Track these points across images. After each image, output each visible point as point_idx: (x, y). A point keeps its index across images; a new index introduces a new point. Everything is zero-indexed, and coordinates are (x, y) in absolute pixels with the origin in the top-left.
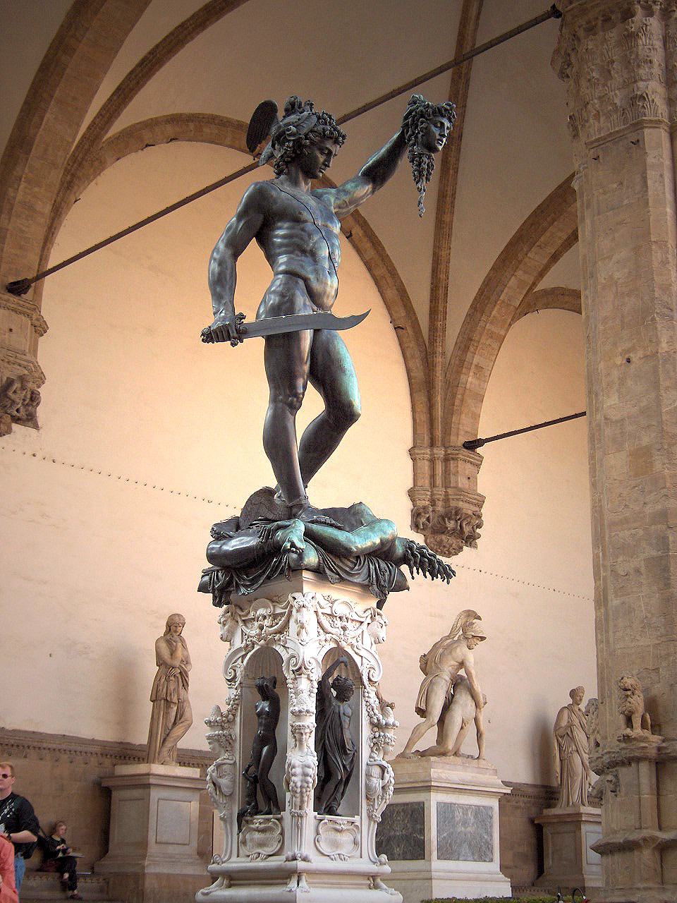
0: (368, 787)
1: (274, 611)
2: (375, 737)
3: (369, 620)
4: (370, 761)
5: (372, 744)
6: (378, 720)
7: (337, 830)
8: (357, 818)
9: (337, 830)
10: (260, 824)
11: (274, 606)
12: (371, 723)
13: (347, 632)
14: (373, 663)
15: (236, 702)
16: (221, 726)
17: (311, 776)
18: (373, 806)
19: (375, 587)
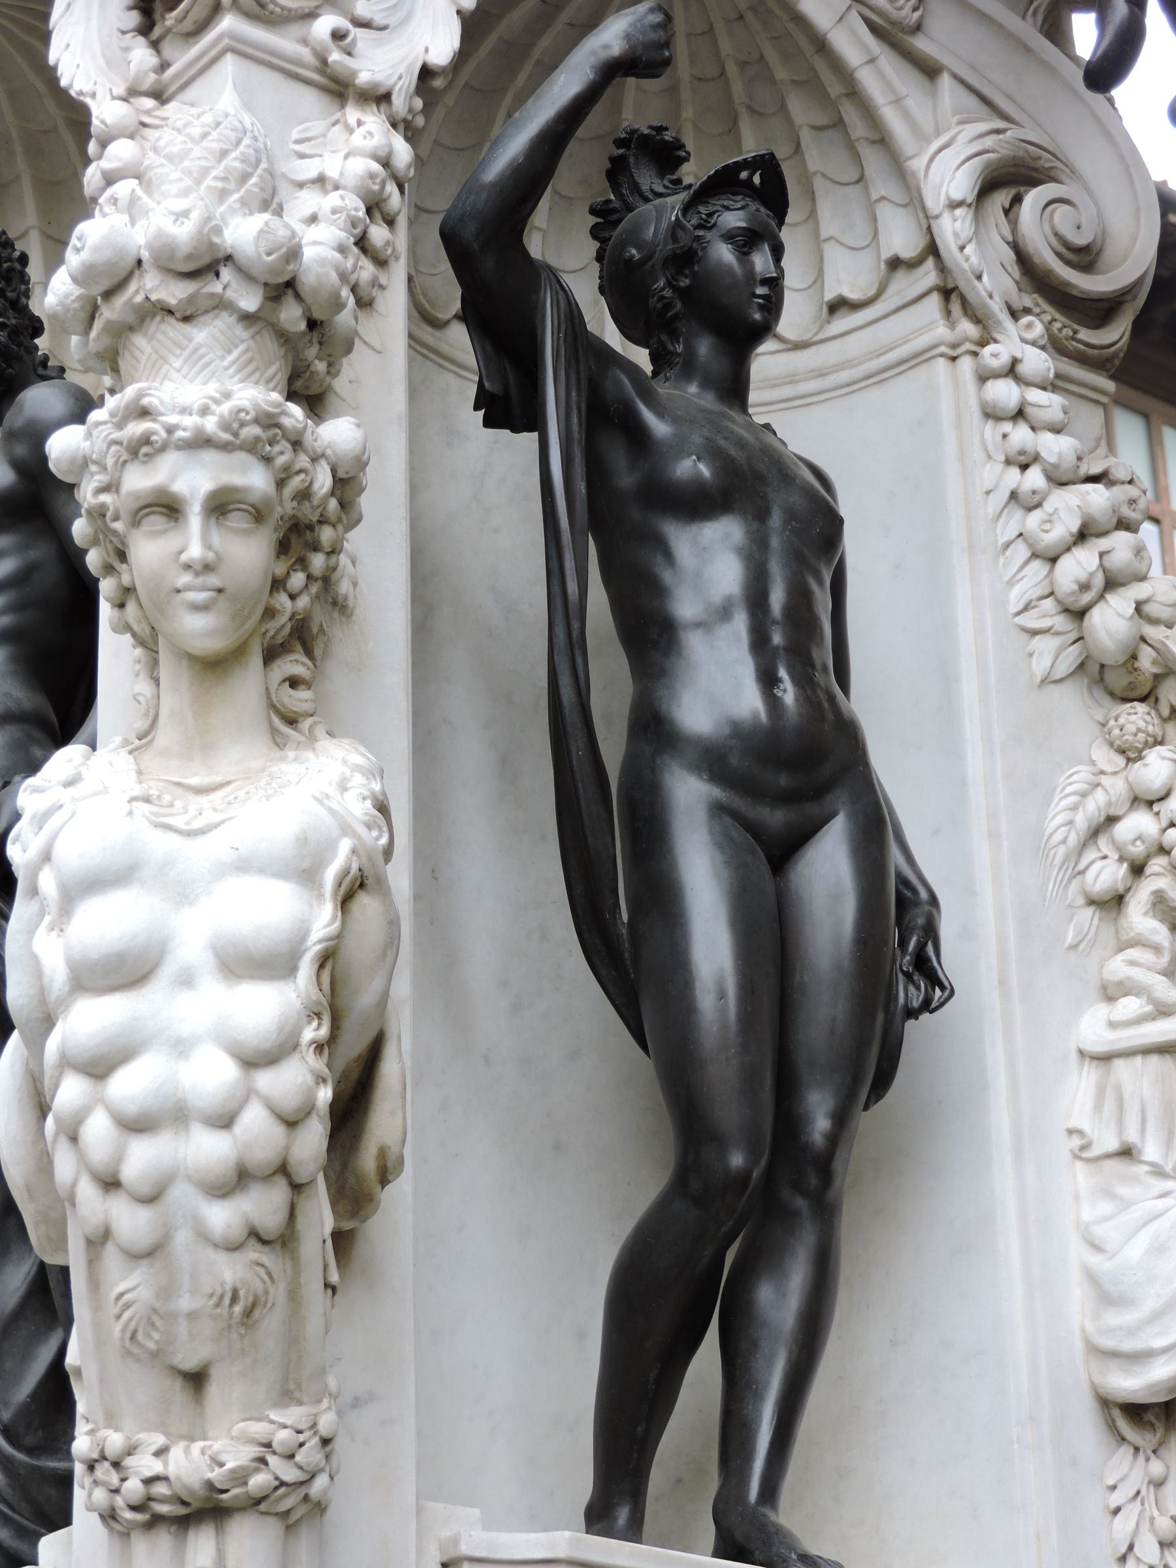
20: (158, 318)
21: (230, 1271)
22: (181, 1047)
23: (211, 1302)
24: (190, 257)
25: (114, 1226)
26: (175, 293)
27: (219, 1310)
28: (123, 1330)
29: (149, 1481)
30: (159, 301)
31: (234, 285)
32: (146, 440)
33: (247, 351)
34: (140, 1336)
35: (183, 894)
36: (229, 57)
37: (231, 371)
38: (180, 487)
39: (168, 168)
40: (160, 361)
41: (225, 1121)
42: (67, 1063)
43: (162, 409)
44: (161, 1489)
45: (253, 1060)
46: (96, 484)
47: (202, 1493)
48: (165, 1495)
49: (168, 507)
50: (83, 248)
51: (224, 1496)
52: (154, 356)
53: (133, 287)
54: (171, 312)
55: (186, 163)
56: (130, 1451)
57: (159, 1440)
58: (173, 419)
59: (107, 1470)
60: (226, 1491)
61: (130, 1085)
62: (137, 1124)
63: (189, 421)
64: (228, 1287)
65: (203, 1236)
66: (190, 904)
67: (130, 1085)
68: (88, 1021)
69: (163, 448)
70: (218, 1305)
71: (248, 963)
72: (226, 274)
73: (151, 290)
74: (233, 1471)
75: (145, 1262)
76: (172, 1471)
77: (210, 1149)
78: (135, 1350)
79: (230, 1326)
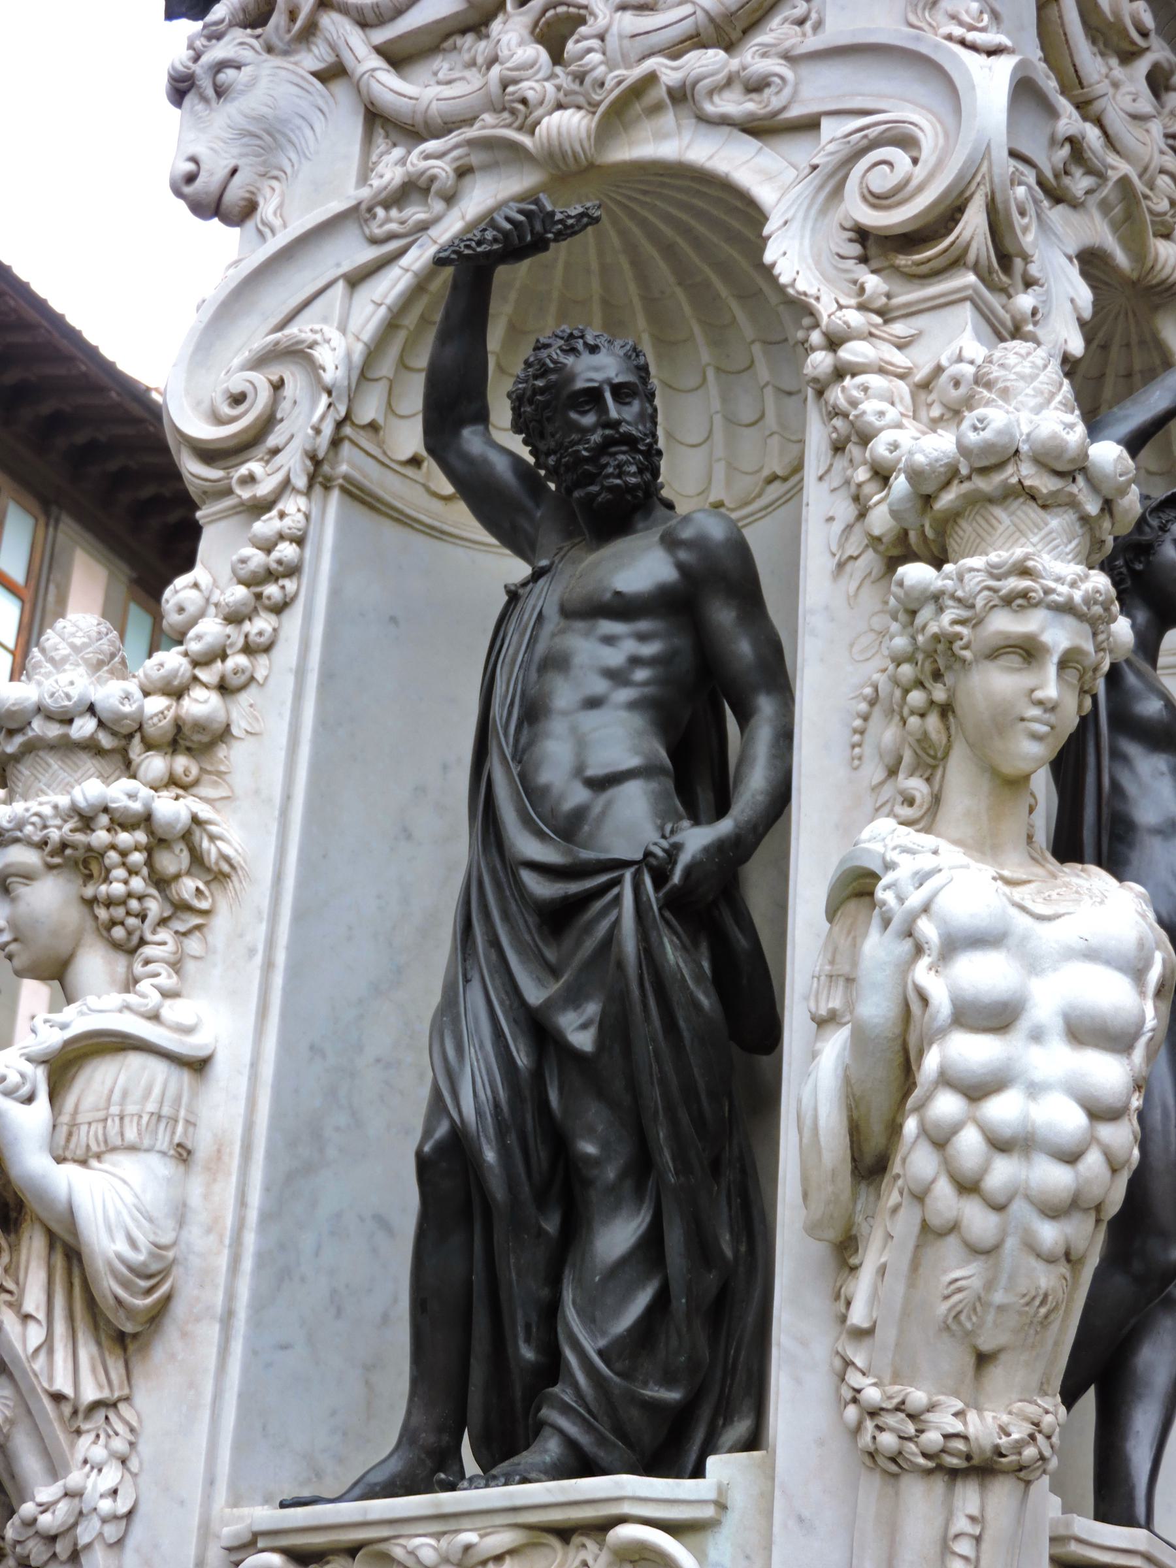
20: (1021, 500)
21: (1045, 1278)
22: (1034, 1090)
23: (1023, 1301)
24: (1072, 461)
25: (965, 1223)
26: (1045, 484)
27: (1027, 1309)
28: (950, 1310)
29: (947, 1437)
30: (1031, 487)
31: (1085, 490)
32: (1024, 594)
33: (1077, 546)
34: (963, 1317)
35: (1033, 965)
36: (968, 304)
37: (1070, 557)
38: (1047, 638)
39: (1021, 384)
40: (1018, 534)
41: (1071, 1158)
42: (946, 1080)
43: (1044, 574)
44: (960, 1445)
45: (1099, 1113)
46: (953, 616)
47: (989, 1454)
48: (960, 1451)
49: (1028, 651)
50: (983, 429)
51: (1003, 1460)
52: (1012, 528)
53: (1010, 469)
54: (1033, 498)
55: (1036, 384)
56: (931, 1407)
57: (959, 1405)
58: (1052, 585)
59: (903, 1420)
60: (1004, 1456)
61: (1003, 1110)
62: (1000, 1144)
63: (1064, 589)
64: (1042, 1292)
65: (1032, 1247)
66: (1037, 975)
67: (1003, 1110)
68: (971, 1051)
69: (1036, 605)
70: (1027, 1304)
71: (1085, 1031)
72: (1080, 480)
73: (1025, 477)
74: (1017, 1441)
75: (983, 1257)
76: (971, 1431)
77: (1053, 1177)
78: (954, 1327)
79: (1032, 1322)
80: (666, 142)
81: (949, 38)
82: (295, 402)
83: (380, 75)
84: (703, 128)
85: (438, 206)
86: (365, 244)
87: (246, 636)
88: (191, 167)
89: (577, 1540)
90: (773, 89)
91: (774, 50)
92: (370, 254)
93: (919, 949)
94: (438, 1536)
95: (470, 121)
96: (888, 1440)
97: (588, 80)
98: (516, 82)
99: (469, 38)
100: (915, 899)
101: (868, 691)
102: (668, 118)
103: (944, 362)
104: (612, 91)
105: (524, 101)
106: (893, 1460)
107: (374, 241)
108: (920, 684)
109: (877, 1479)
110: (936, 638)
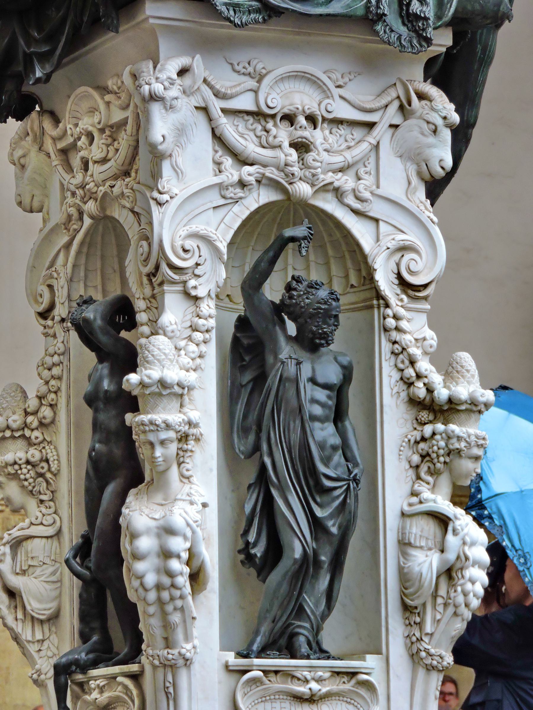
0: (405, 578)
1: (109, 116)
2: (423, 439)
3: (392, 115)
4: (410, 505)
5: (416, 459)
6: (430, 390)
7: (299, 698)
8: (372, 661)
9: (299, 698)
10: (101, 691)
11: (108, 103)
12: (414, 402)
13: (310, 157)
14: (412, 236)
15: (56, 371)
16: (23, 436)
17: (178, 557)
18: (420, 625)
19: (393, 19)
36: (426, 314)
80: (329, 205)
81: (429, 217)
82: (205, 260)
83: (227, 125)
84: (339, 204)
85: (248, 193)
86: (220, 197)
87: (201, 352)
88: (162, 139)
89: (341, 675)
90: (367, 204)
91: (369, 189)
92: (222, 202)
93: (464, 543)
94: (310, 672)
95: (265, 166)
96: (435, 663)
97: (316, 177)
98: (292, 166)
99: (251, 120)
100: (466, 531)
101: (406, 440)
102: (330, 196)
103: (428, 337)
104: (321, 182)
105: (293, 174)
106: (433, 667)
107: (224, 197)
108: (443, 456)
109: (425, 670)
110: (457, 449)
